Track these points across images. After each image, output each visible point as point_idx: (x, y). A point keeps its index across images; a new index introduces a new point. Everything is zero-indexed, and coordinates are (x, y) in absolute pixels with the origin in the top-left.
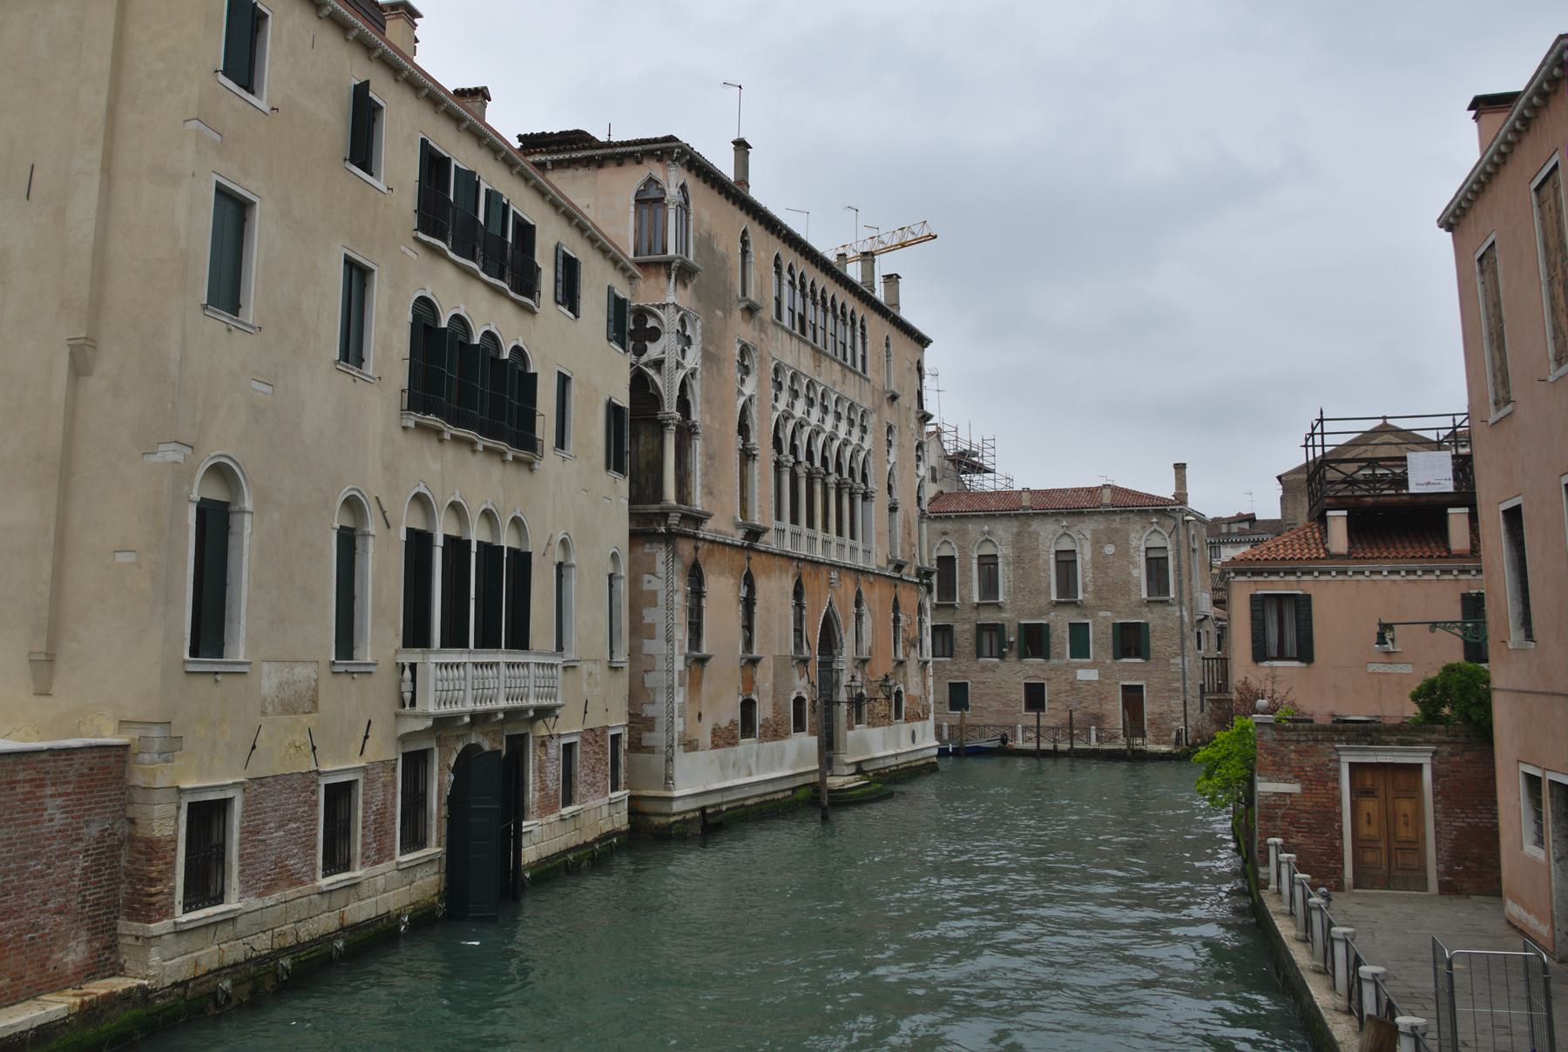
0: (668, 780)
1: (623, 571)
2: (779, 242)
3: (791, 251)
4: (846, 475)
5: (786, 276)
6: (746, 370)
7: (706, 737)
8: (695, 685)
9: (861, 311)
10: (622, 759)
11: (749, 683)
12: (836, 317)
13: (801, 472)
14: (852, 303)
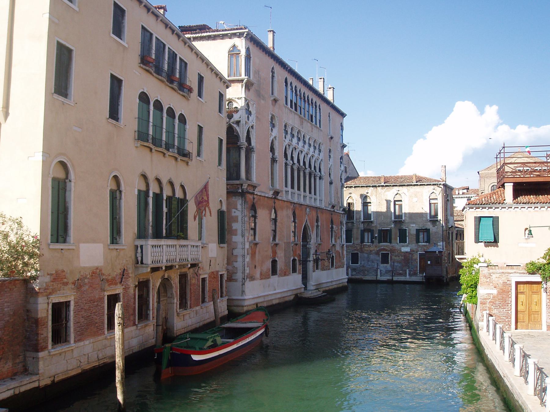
2: (286, 72)
3: (292, 76)
4: (313, 169)
6: (273, 126)
7: (258, 275)
8: (253, 255)
9: (319, 102)
11: (274, 253)
12: (309, 104)
13: (295, 167)
14: (315, 99)
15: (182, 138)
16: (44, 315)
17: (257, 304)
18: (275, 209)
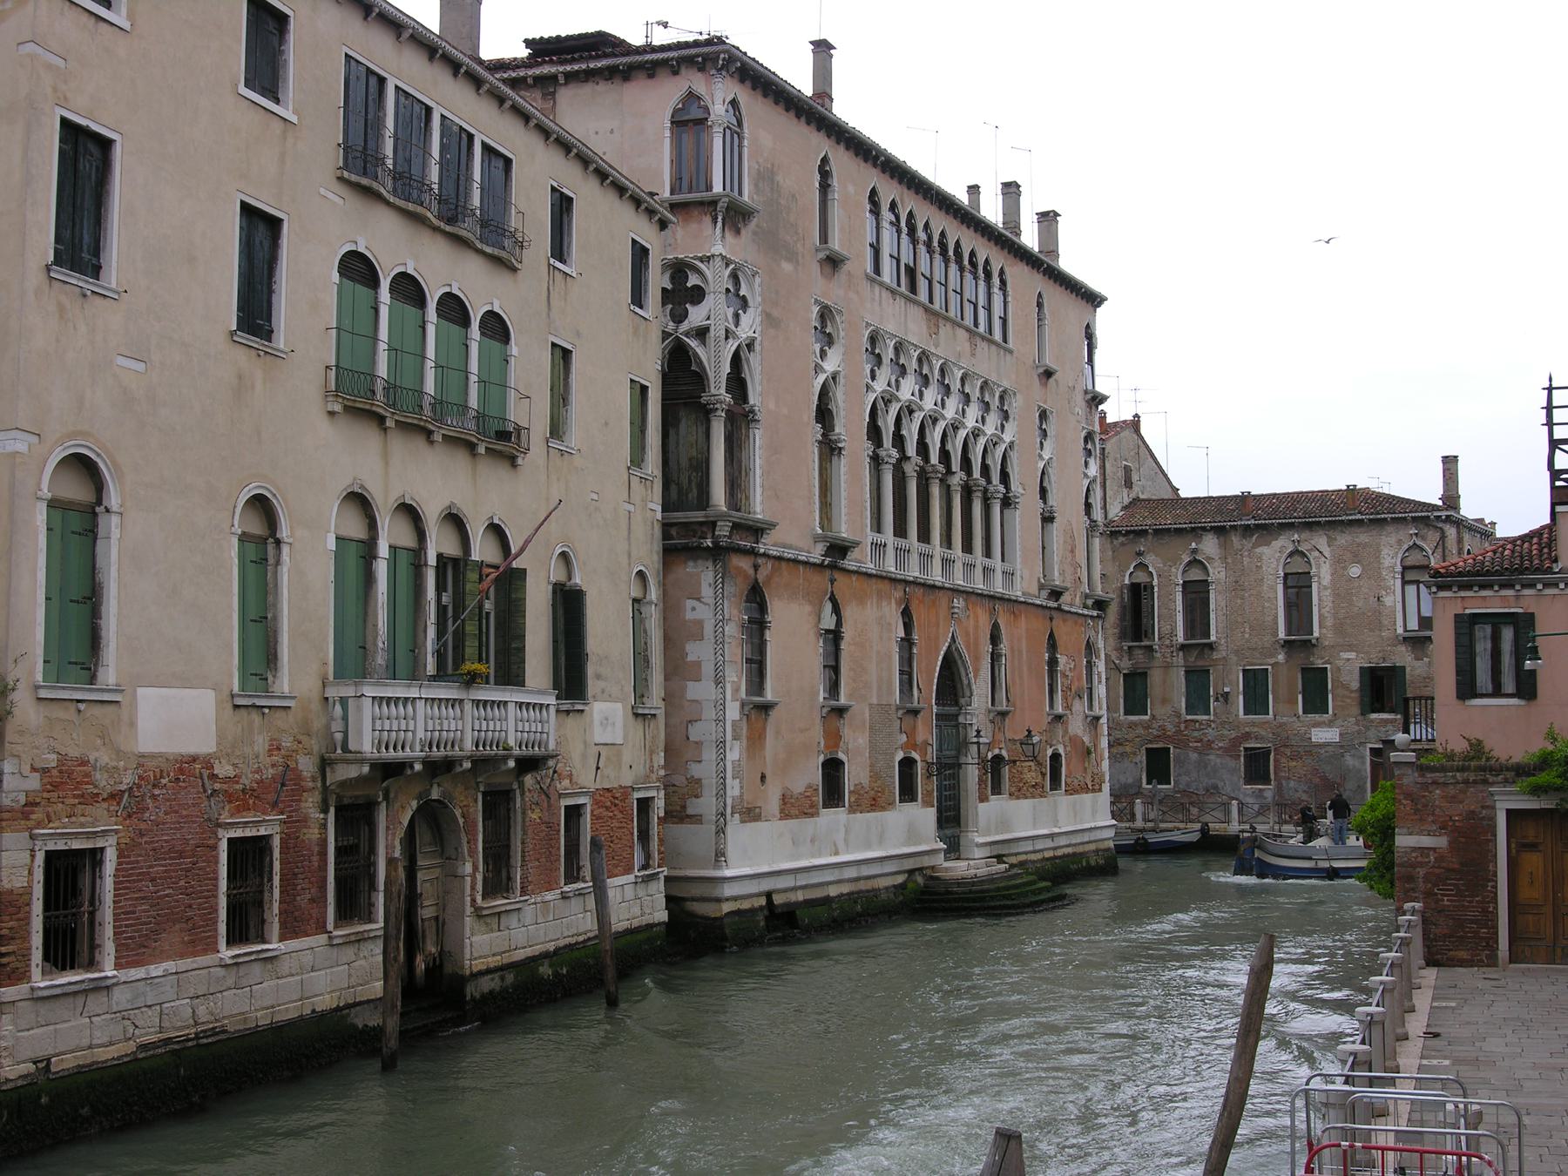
0: (720, 856)
1: (654, 594)
3: (895, 183)
4: (977, 473)
5: (887, 216)
7: (773, 804)
8: (755, 740)
9: (998, 260)
10: (655, 828)
11: (834, 738)
13: (910, 469)
14: (985, 251)
15: (495, 383)
17: (769, 895)
18: (833, 599)
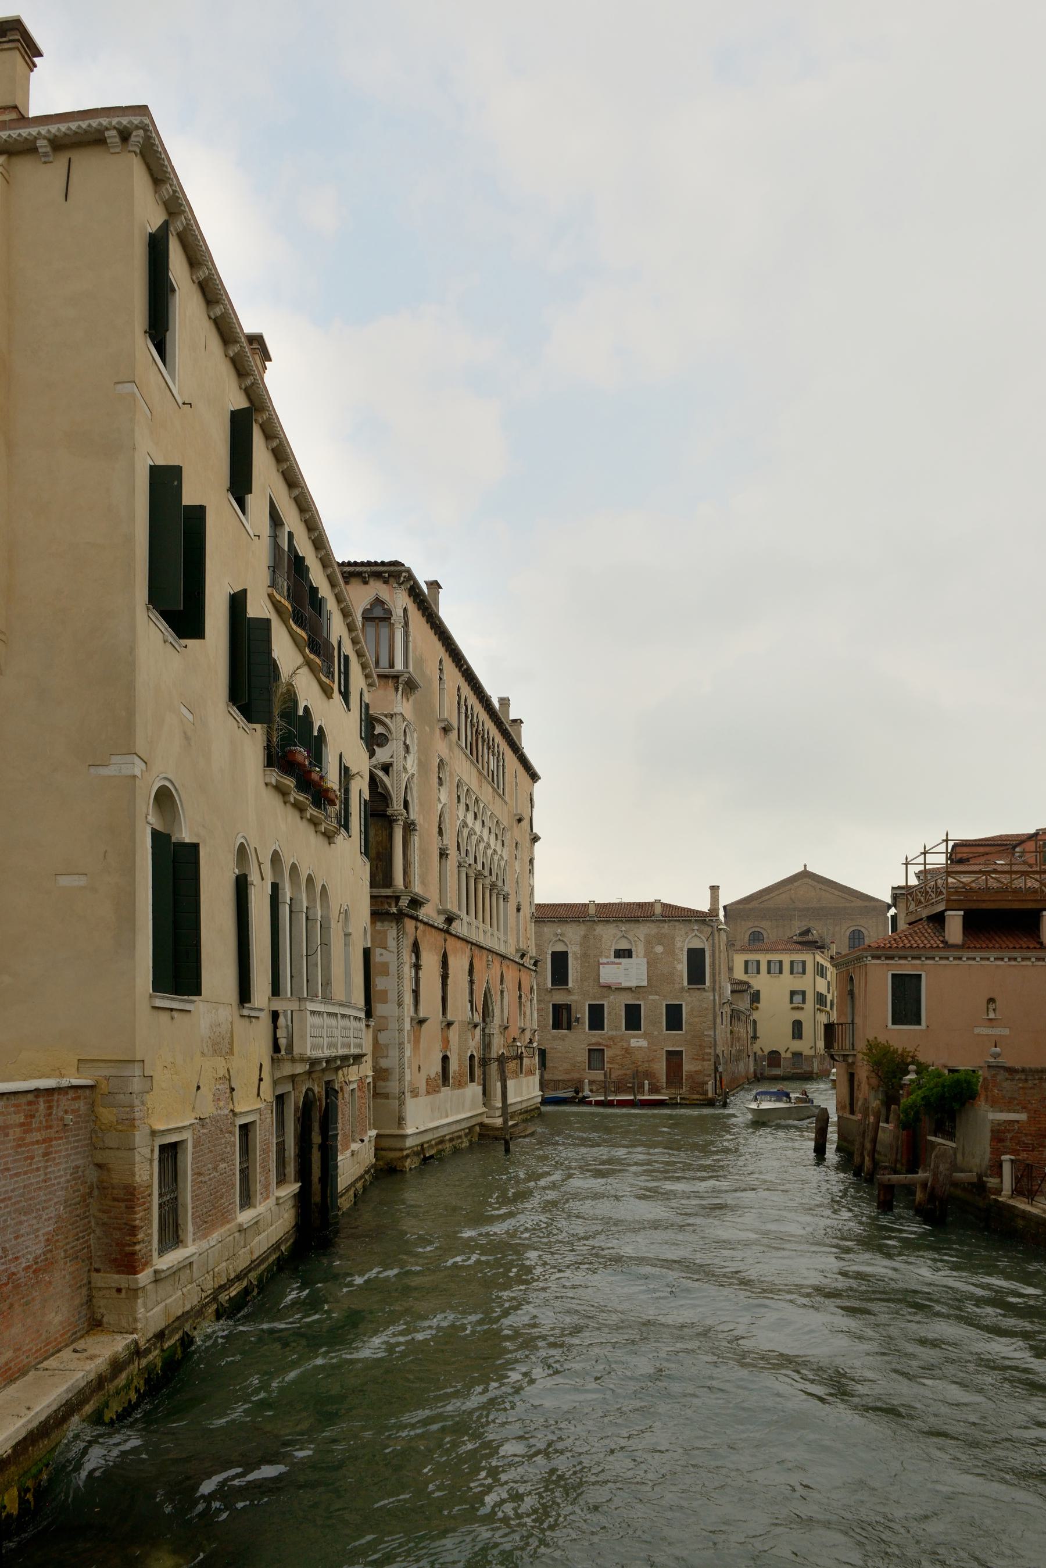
0: (401, 1121)
11: (446, 1042)
16: (146, 1178)
